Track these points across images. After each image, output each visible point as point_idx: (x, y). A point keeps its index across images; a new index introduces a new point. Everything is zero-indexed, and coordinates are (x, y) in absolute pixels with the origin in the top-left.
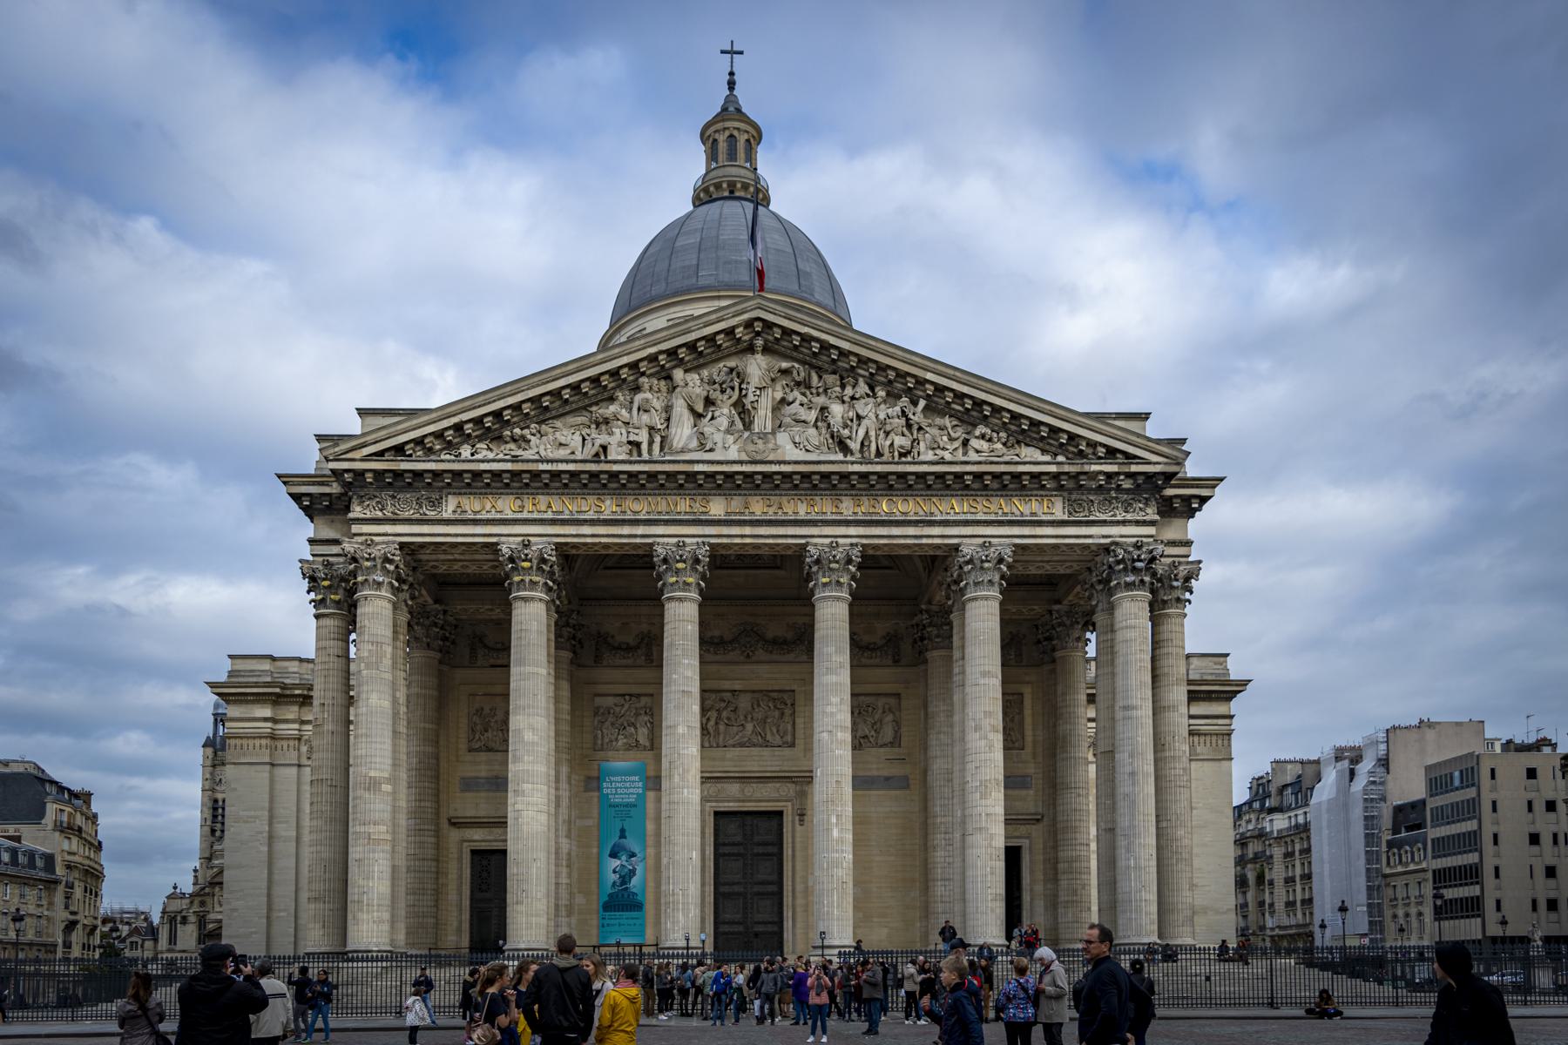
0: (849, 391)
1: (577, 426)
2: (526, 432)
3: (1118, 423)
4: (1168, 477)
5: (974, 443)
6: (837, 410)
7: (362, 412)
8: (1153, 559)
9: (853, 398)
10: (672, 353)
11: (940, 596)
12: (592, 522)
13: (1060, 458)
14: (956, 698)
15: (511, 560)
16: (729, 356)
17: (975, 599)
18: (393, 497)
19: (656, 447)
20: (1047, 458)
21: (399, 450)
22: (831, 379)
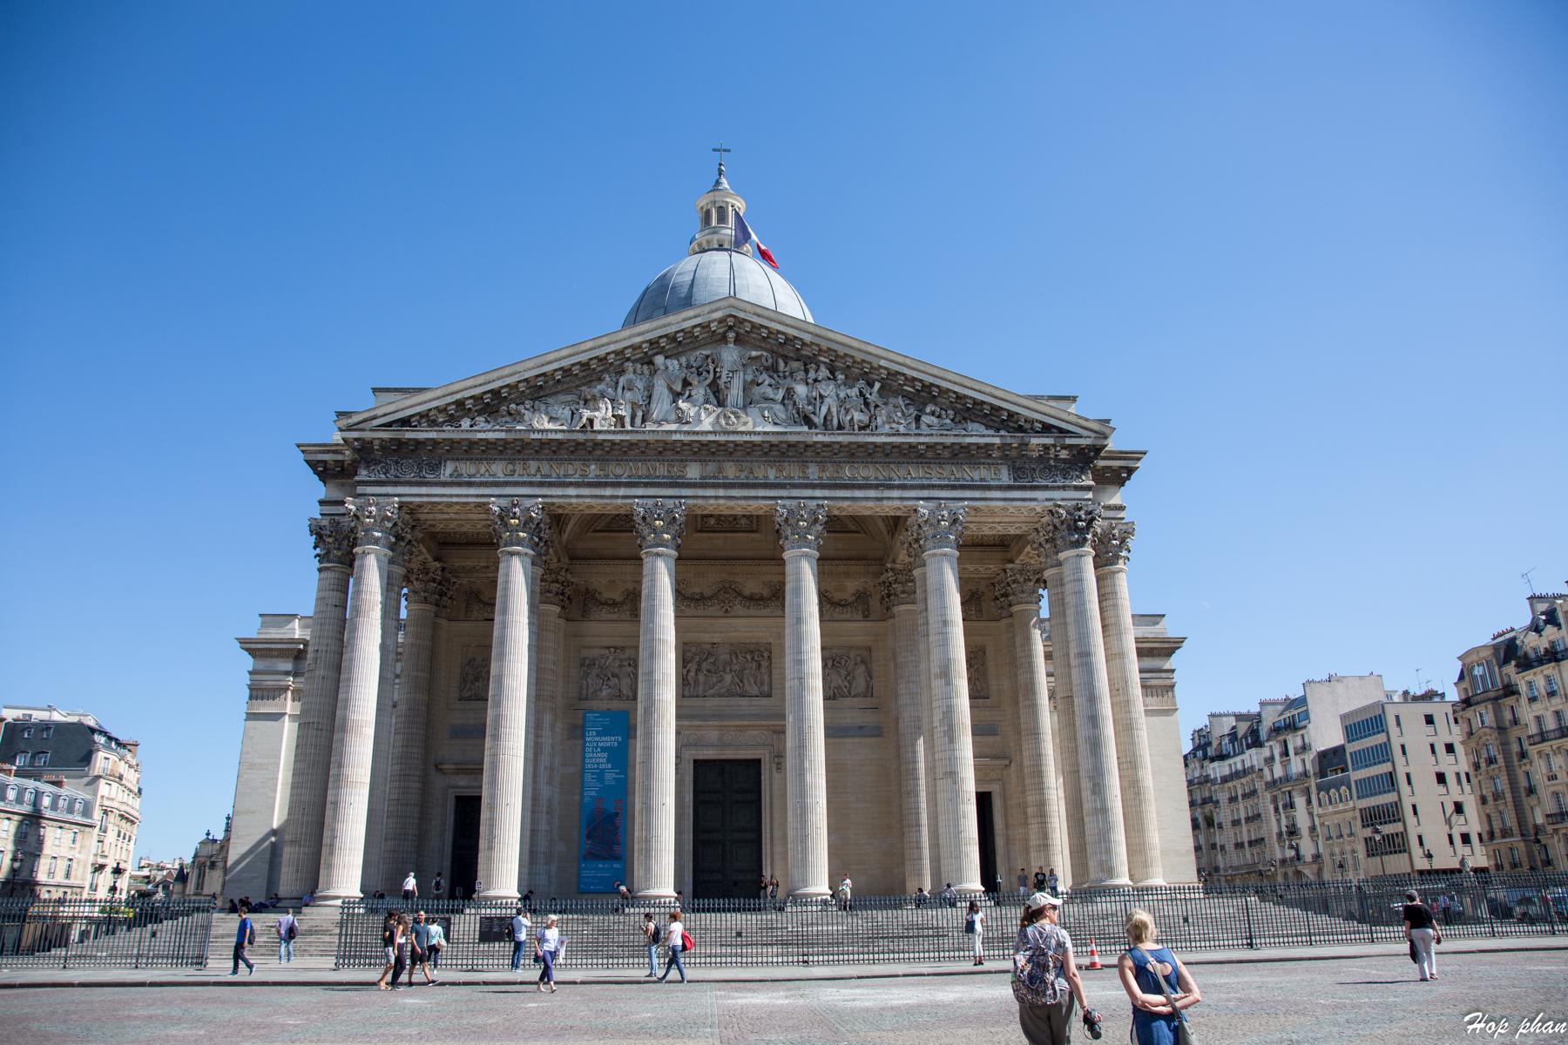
0: (812, 375)
1: (567, 403)
2: (521, 407)
3: (1053, 403)
4: (1098, 450)
5: (925, 419)
6: (801, 390)
7: (375, 390)
8: (1090, 522)
9: (816, 380)
10: (653, 343)
11: (903, 557)
12: (577, 485)
13: (1002, 433)
14: (921, 647)
15: (501, 518)
16: (704, 345)
17: (934, 555)
18: (397, 462)
19: (638, 420)
20: (991, 432)
21: (405, 422)
22: (795, 365)
